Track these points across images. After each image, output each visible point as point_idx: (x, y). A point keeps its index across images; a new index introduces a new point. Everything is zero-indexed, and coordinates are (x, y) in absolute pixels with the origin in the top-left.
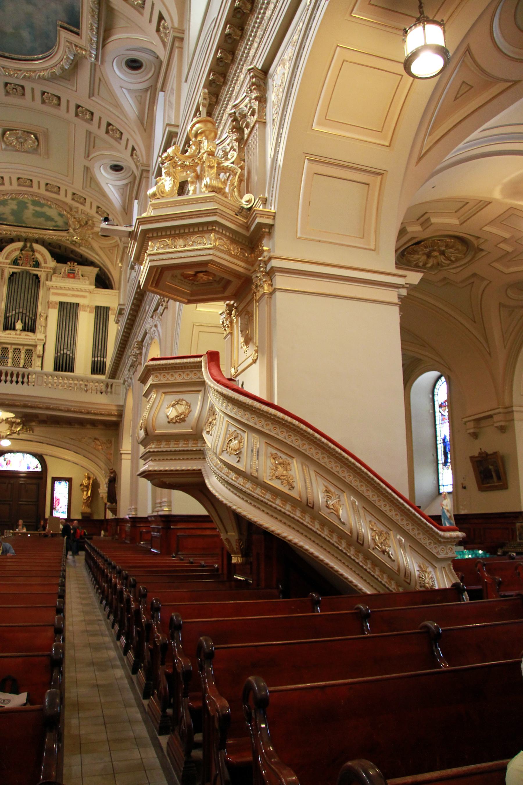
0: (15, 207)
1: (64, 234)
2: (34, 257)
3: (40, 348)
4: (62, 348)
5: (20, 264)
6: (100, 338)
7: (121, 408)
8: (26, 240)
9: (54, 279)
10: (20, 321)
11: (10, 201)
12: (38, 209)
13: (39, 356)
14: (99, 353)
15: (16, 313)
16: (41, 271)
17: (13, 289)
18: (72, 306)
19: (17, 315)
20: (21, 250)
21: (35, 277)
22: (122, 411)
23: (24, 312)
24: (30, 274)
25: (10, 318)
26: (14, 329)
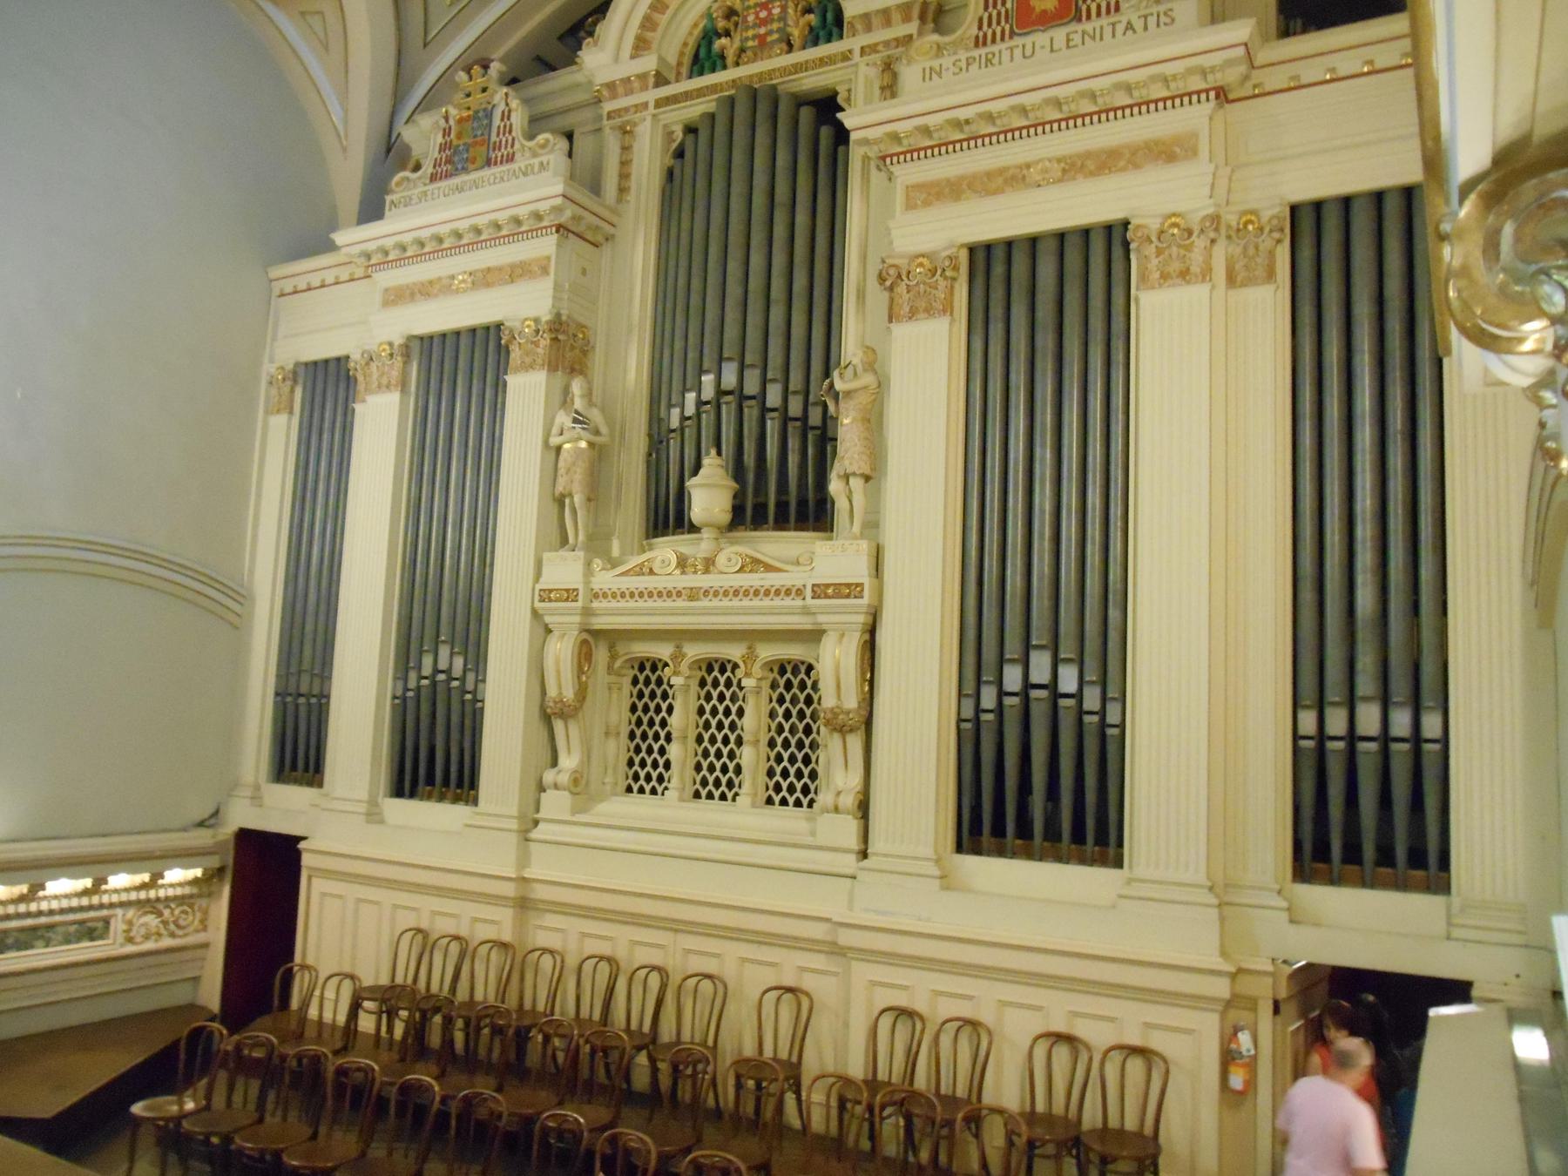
4: (1013, 648)
6: (1365, 502)
9: (910, 75)
10: (710, 462)
14: (1366, 661)
15: (700, 403)
16: (846, 56)
21: (806, 114)
23: (751, 387)
25: (674, 445)
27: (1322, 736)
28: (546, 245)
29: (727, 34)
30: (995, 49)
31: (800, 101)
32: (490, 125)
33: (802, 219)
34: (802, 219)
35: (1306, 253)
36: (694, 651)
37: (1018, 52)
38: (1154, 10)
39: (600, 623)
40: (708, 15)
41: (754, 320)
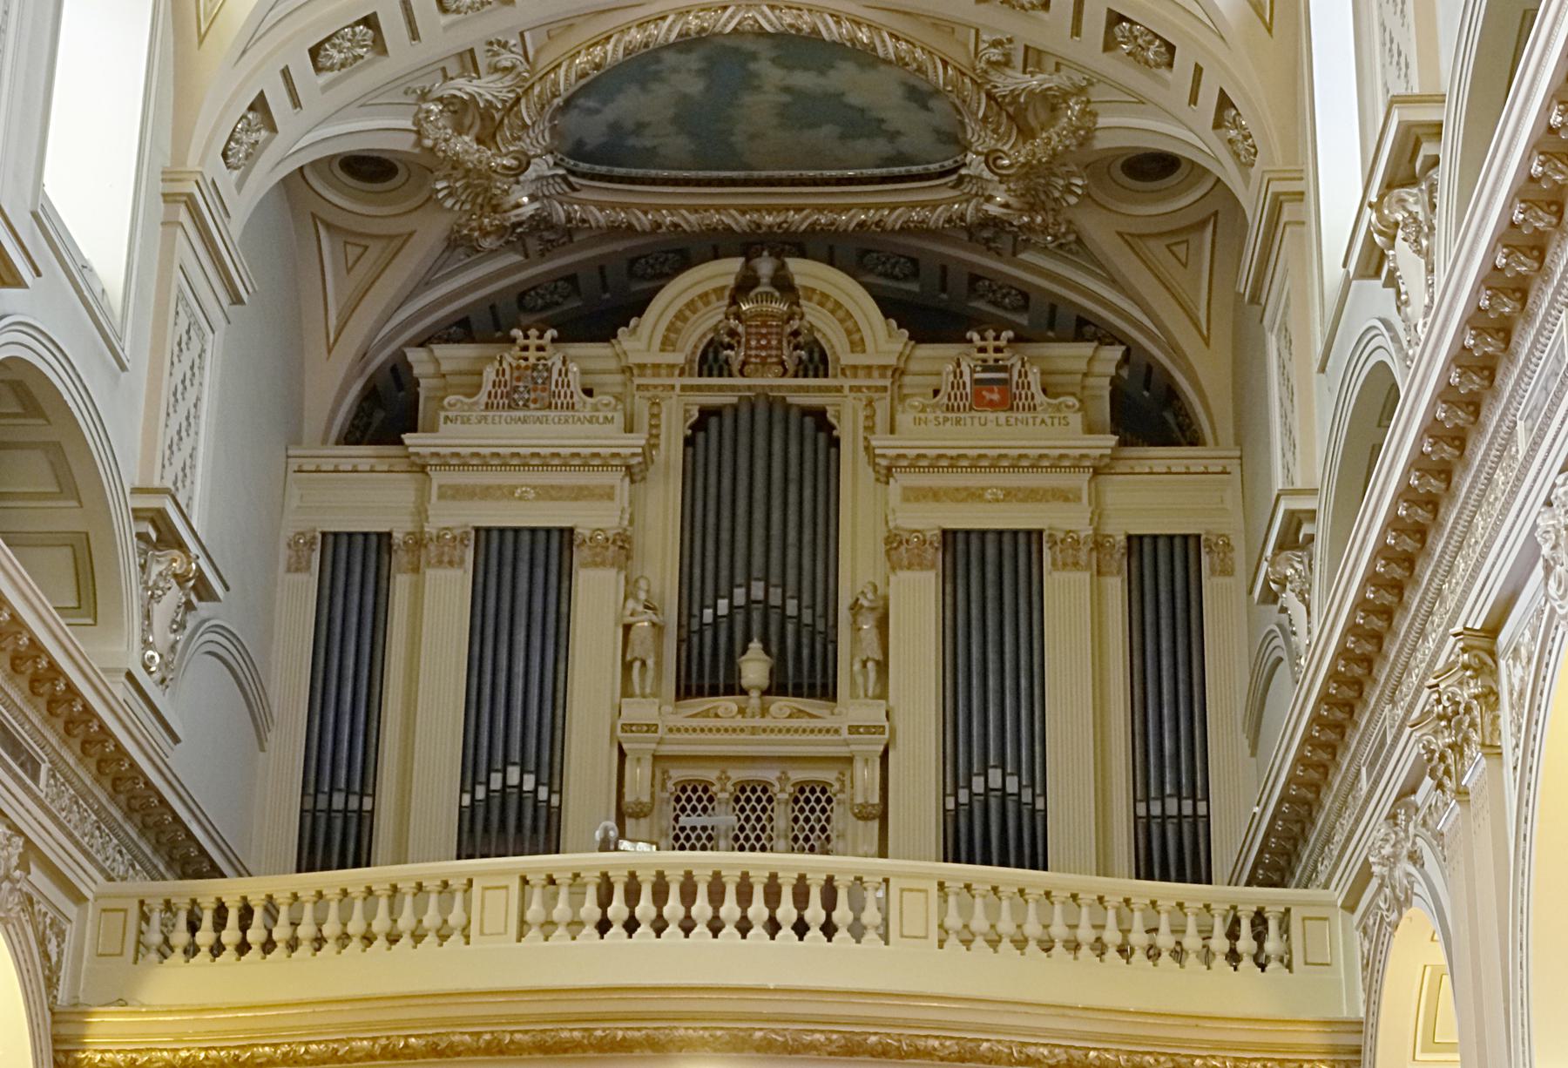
0: (695, 87)
1: (941, 192)
2: (795, 324)
3: (866, 776)
5: (736, 368)
7: (1349, 1040)
8: (748, 245)
9: (905, 419)
10: (756, 645)
11: (670, 58)
12: (804, 80)
13: (863, 816)
15: (731, 606)
17: (712, 490)
18: (1007, 548)
19: (739, 618)
20: (734, 301)
21: (809, 421)
22: (1358, 1051)
23: (775, 599)
24: (787, 408)
26: (733, 687)
27: (1149, 816)
28: (616, 478)
29: (731, 347)
30: (962, 415)
31: (806, 411)
32: (550, 377)
33: (808, 493)
34: (808, 493)
35: (1134, 564)
36: (738, 774)
37: (976, 421)
38: (1057, 415)
39: (665, 750)
40: (715, 329)
41: (775, 554)
